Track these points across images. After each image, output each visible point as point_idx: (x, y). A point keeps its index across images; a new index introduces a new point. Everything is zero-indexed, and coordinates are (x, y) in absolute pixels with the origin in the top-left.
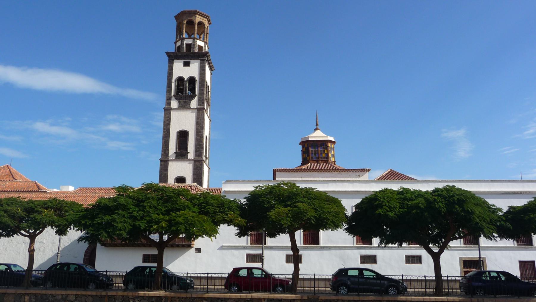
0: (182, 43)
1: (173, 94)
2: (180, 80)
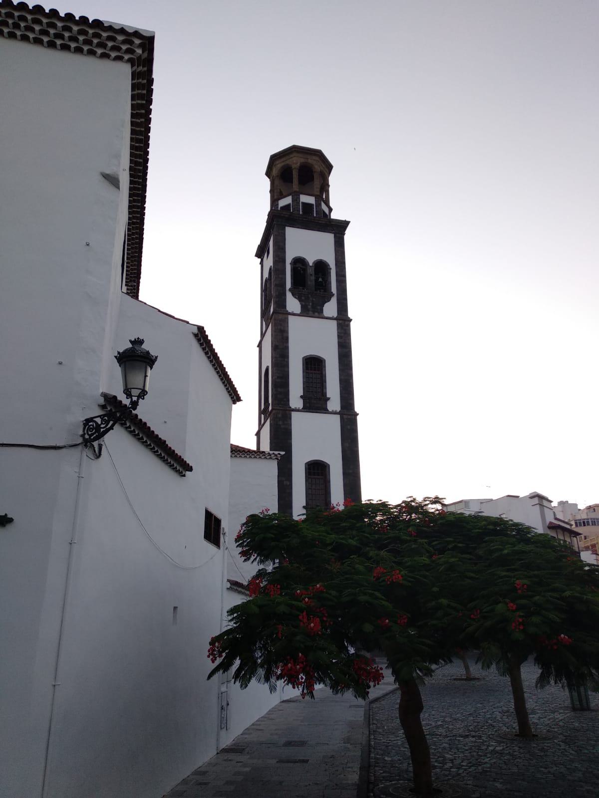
0: (296, 200)
1: (289, 285)
2: (299, 262)
